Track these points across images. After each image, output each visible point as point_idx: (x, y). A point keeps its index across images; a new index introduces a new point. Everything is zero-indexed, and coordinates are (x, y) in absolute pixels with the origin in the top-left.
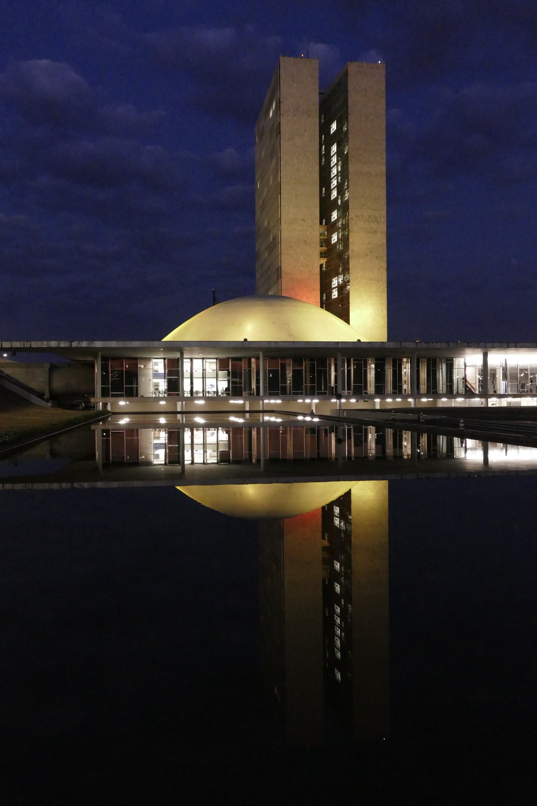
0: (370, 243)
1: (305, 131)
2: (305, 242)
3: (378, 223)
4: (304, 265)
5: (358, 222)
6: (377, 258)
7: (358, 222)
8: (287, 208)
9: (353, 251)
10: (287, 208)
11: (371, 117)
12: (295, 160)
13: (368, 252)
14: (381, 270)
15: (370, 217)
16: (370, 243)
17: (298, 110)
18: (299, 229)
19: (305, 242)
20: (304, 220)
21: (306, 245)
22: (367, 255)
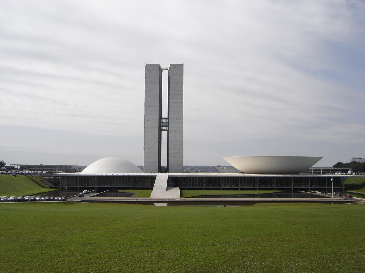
0: (177, 127)
1: (154, 89)
2: (153, 127)
5: (173, 120)
6: (179, 132)
7: (173, 120)
8: (147, 115)
9: (170, 130)
10: (147, 115)
13: (176, 130)
15: (177, 118)
16: (177, 127)
17: (151, 81)
18: (151, 123)
19: (153, 127)
20: (153, 120)
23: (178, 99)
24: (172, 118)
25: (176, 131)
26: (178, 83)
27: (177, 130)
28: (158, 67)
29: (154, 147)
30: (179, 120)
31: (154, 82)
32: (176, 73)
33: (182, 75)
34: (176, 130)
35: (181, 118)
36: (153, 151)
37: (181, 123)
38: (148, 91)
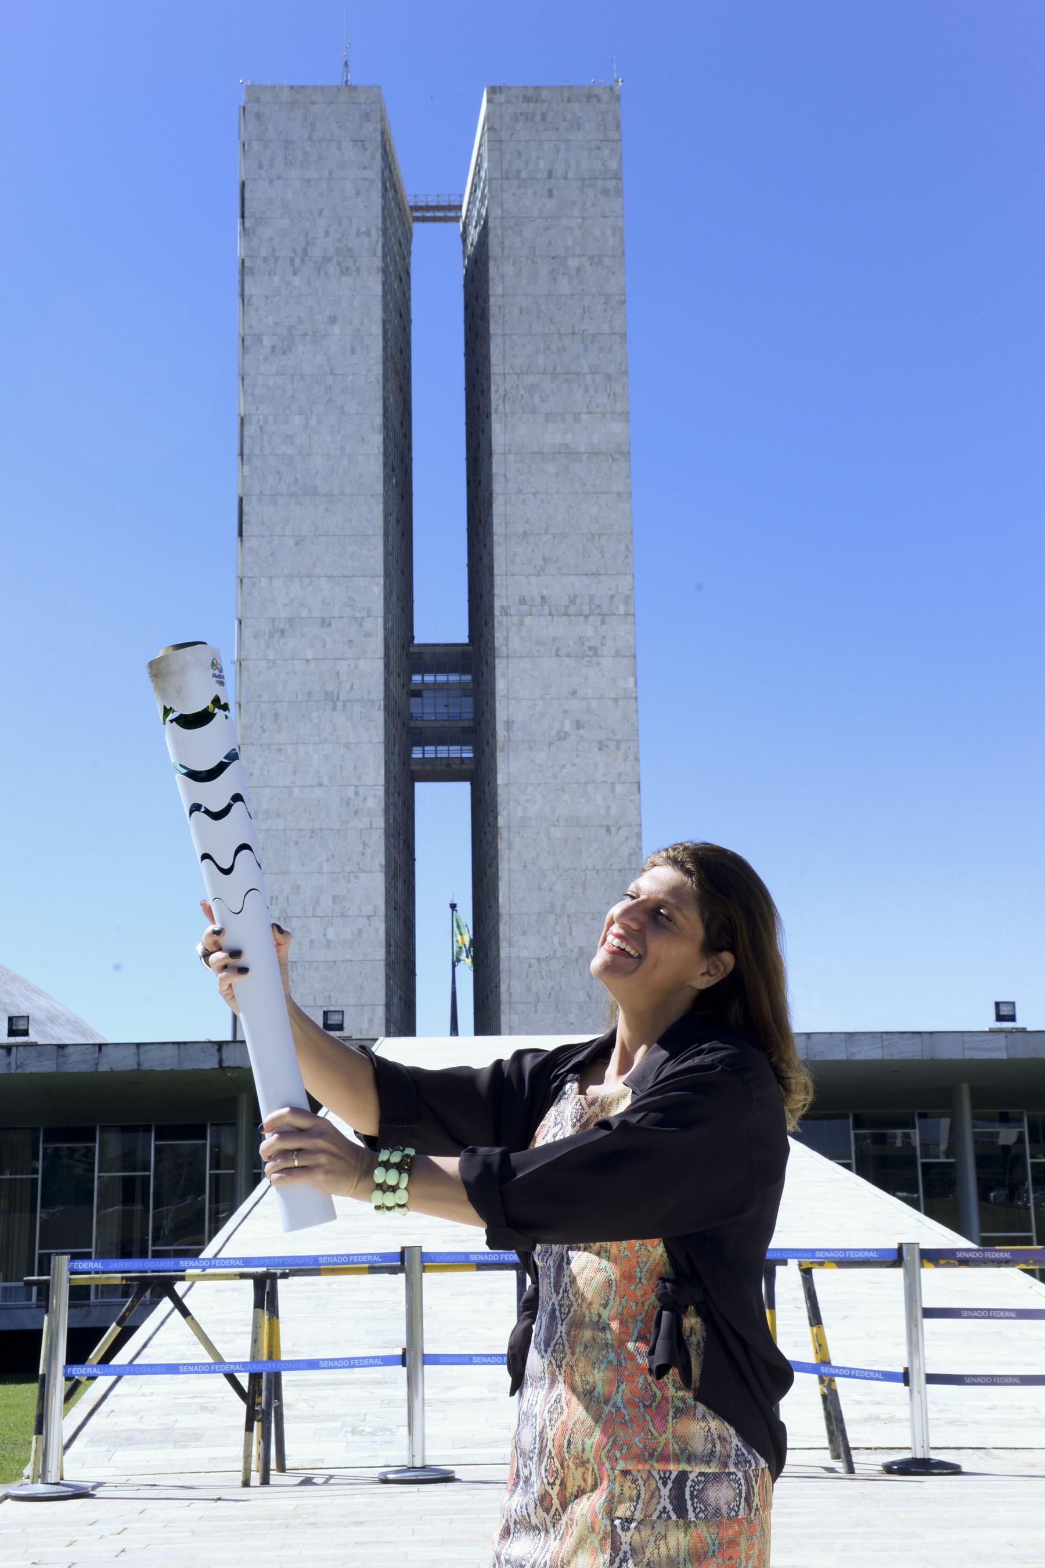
0: (574, 693)
1: (333, 320)
3: (603, 623)
4: (326, 781)
5: (528, 620)
7: (528, 620)
8: (264, 583)
9: (509, 724)
10: (264, 583)
11: (573, 263)
12: (297, 420)
13: (568, 726)
14: (619, 789)
15: (572, 601)
17: (305, 251)
18: (309, 656)
19: (331, 699)
21: (334, 709)
22: (563, 736)
23: (577, 418)
24: (522, 601)
25: (563, 736)
26: (573, 263)
27: (579, 725)
28: (366, 117)
29: (335, 898)
30: (595, 620)
31: (327, 260)
32: (550, 175)
33: (606, 192)
34: (568, 726)
35: (612, 597)
36: (329, 943)
37: (617, 654)
38: (267, 341)
